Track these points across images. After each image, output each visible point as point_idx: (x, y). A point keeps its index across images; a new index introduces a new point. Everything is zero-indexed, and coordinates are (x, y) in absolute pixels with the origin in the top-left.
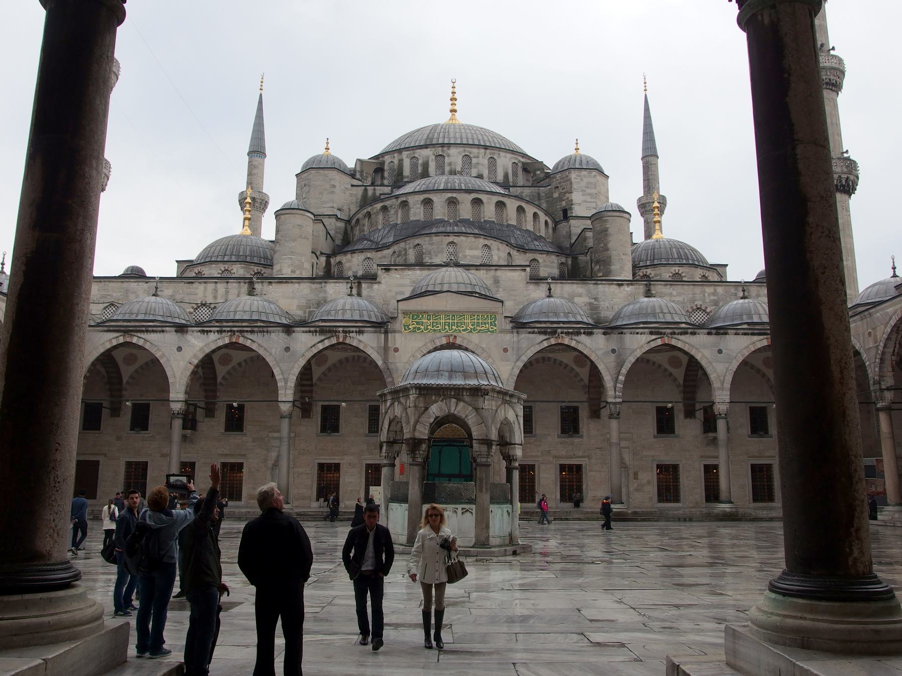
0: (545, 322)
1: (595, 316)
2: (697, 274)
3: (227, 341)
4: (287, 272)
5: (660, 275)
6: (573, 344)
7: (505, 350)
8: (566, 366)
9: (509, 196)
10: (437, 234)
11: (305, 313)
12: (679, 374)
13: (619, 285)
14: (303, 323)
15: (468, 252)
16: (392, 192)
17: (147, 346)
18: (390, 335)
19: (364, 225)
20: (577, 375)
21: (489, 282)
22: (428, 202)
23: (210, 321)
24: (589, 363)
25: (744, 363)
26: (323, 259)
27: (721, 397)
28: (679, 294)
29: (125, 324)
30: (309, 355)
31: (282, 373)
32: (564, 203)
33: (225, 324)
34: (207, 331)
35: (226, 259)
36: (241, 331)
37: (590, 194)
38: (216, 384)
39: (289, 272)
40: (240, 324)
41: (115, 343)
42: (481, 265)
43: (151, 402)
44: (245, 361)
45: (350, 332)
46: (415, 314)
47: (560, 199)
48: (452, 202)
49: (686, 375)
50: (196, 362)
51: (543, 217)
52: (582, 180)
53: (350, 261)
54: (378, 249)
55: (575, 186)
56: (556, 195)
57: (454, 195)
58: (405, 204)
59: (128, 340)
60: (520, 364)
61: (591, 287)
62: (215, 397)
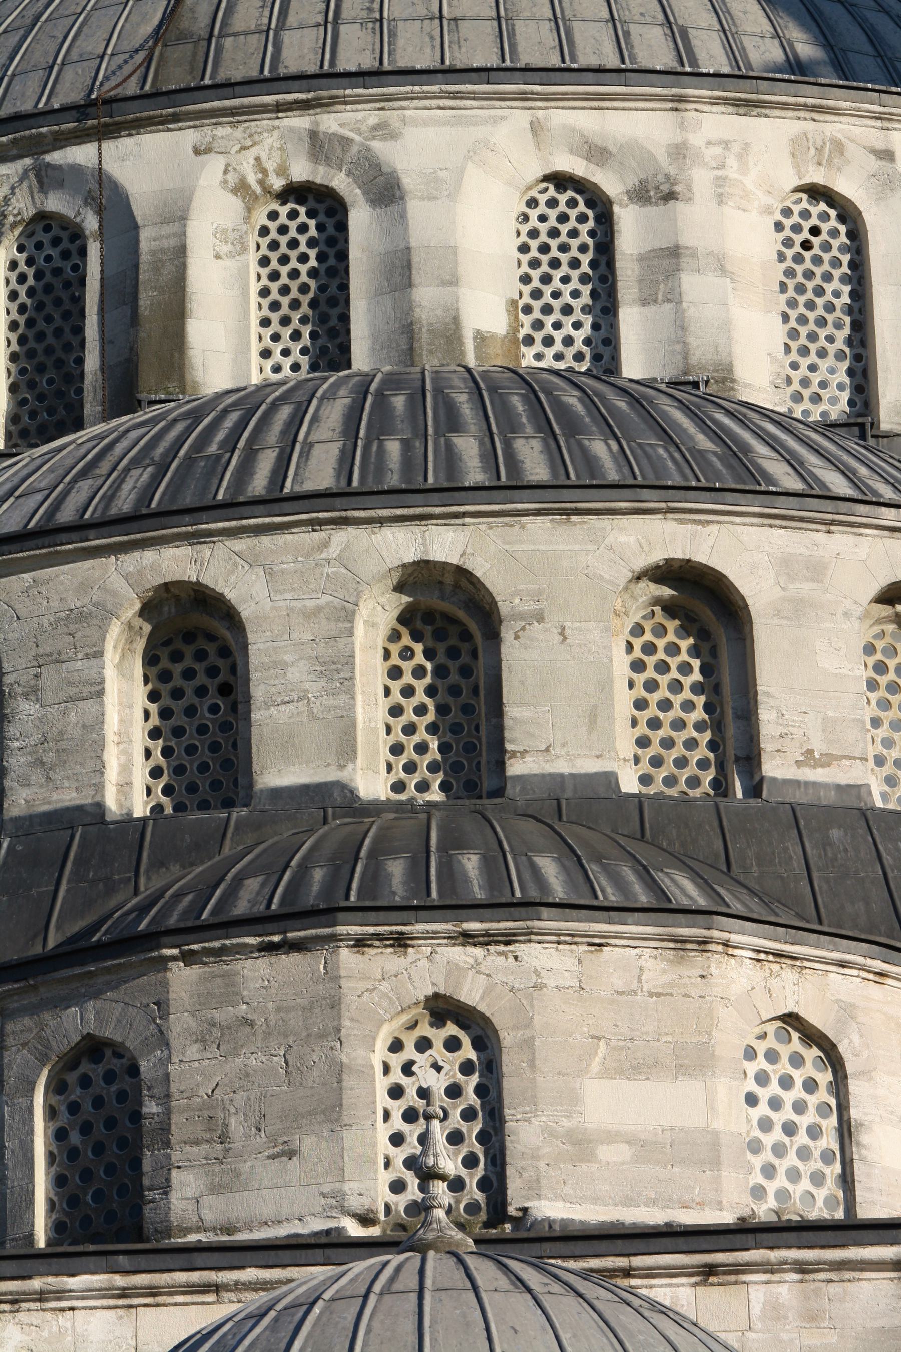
15: (610, 1104)
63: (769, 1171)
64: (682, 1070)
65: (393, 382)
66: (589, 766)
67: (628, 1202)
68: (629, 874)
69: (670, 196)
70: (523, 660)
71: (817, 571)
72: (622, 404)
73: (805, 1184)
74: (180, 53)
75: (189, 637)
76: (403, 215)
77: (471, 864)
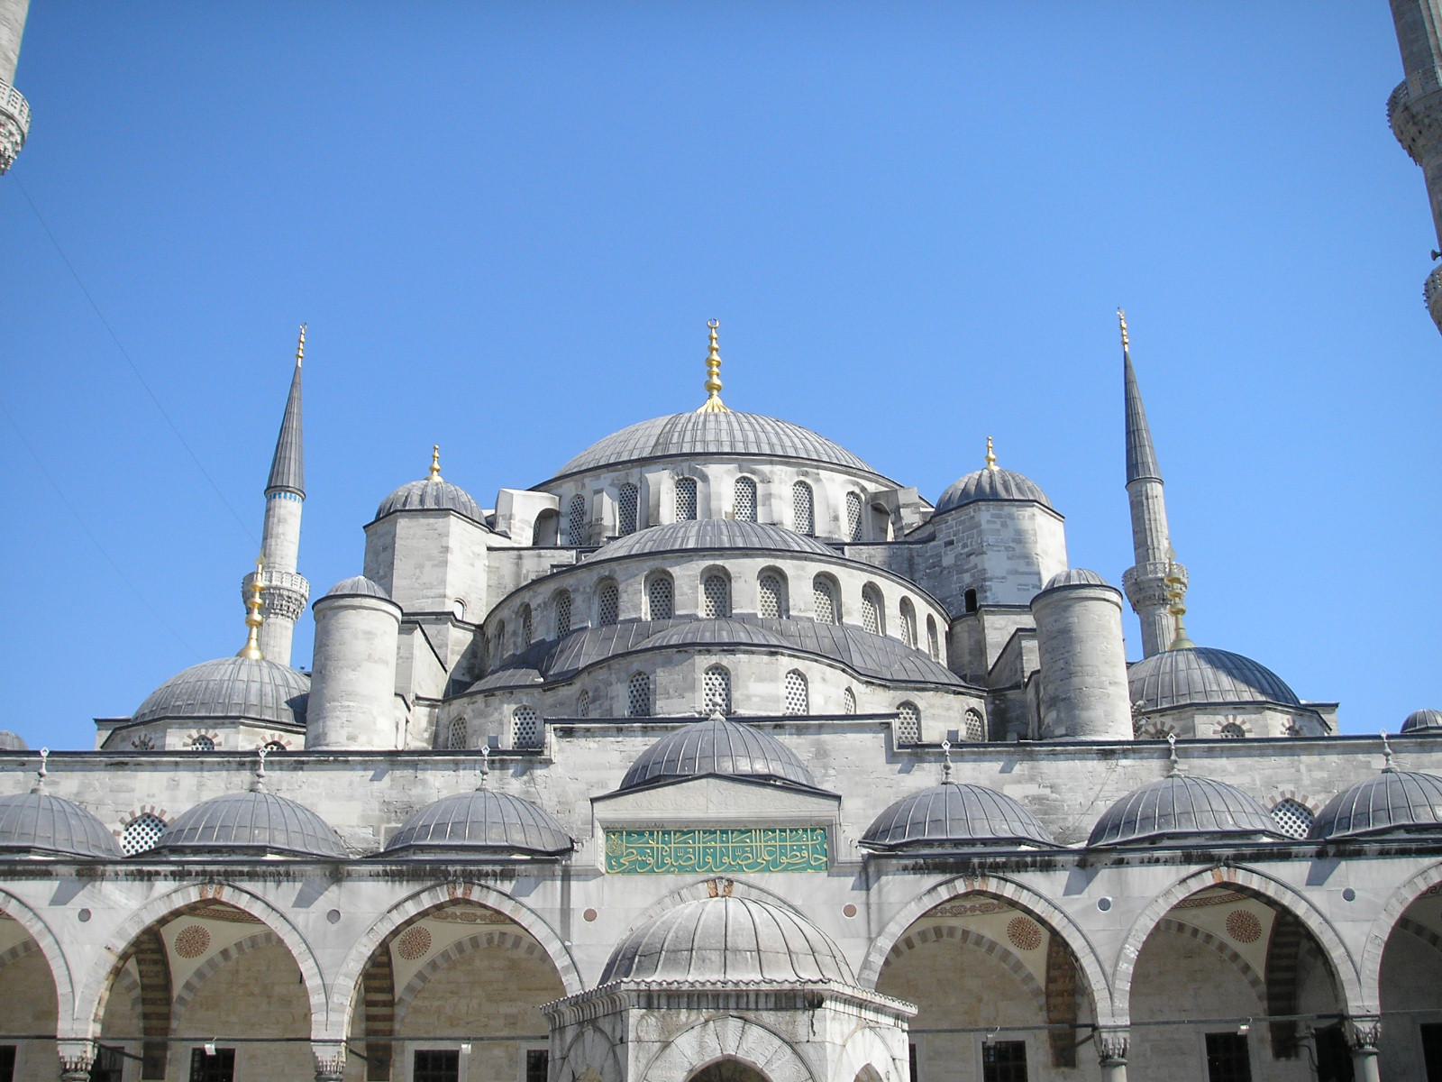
0: (941, 843)
1: (1055, 828)
2: (1277, 723)
3: (193, 895)
4: (338, 739)
5: (1194, 729)
6: (1009, 891)
7: (850, 911)
8: (992, 946)
9: (844, 562)
12: (1256, 954)
14: (372, 858)
18: (574, 884)
20: (1018, 966)
23: (155, 851)
24: (1045, 935)
25: (1403, 922)
26: (421, 713)
27: (1363, 999)
30: (385, 929)
32: (967, 578)
36: (227, 874)
38: (168, 1001)
44: (239, 945)
45: (482, 875)
49: (1271, 957)
50: (121, 945)
51: (922, 608)
52: (1004, 525)
53: (481, 714)
55: (991, 539)
57: (720, 562)
60: (886, 943)
62: (166, 1030)
63: (790, 703)
64: (772, 681)
65: (707, 524)
66: (752, 612)
67: (759, 710)
68: (760, 637)
69: (769, 482)
70: (737, 587)
71: (803, 569)
72: (759, 529)
73: (798, 706)
74: (660, 447)
75: (661, 580)
76: (709, 484)
77: (724, 633)
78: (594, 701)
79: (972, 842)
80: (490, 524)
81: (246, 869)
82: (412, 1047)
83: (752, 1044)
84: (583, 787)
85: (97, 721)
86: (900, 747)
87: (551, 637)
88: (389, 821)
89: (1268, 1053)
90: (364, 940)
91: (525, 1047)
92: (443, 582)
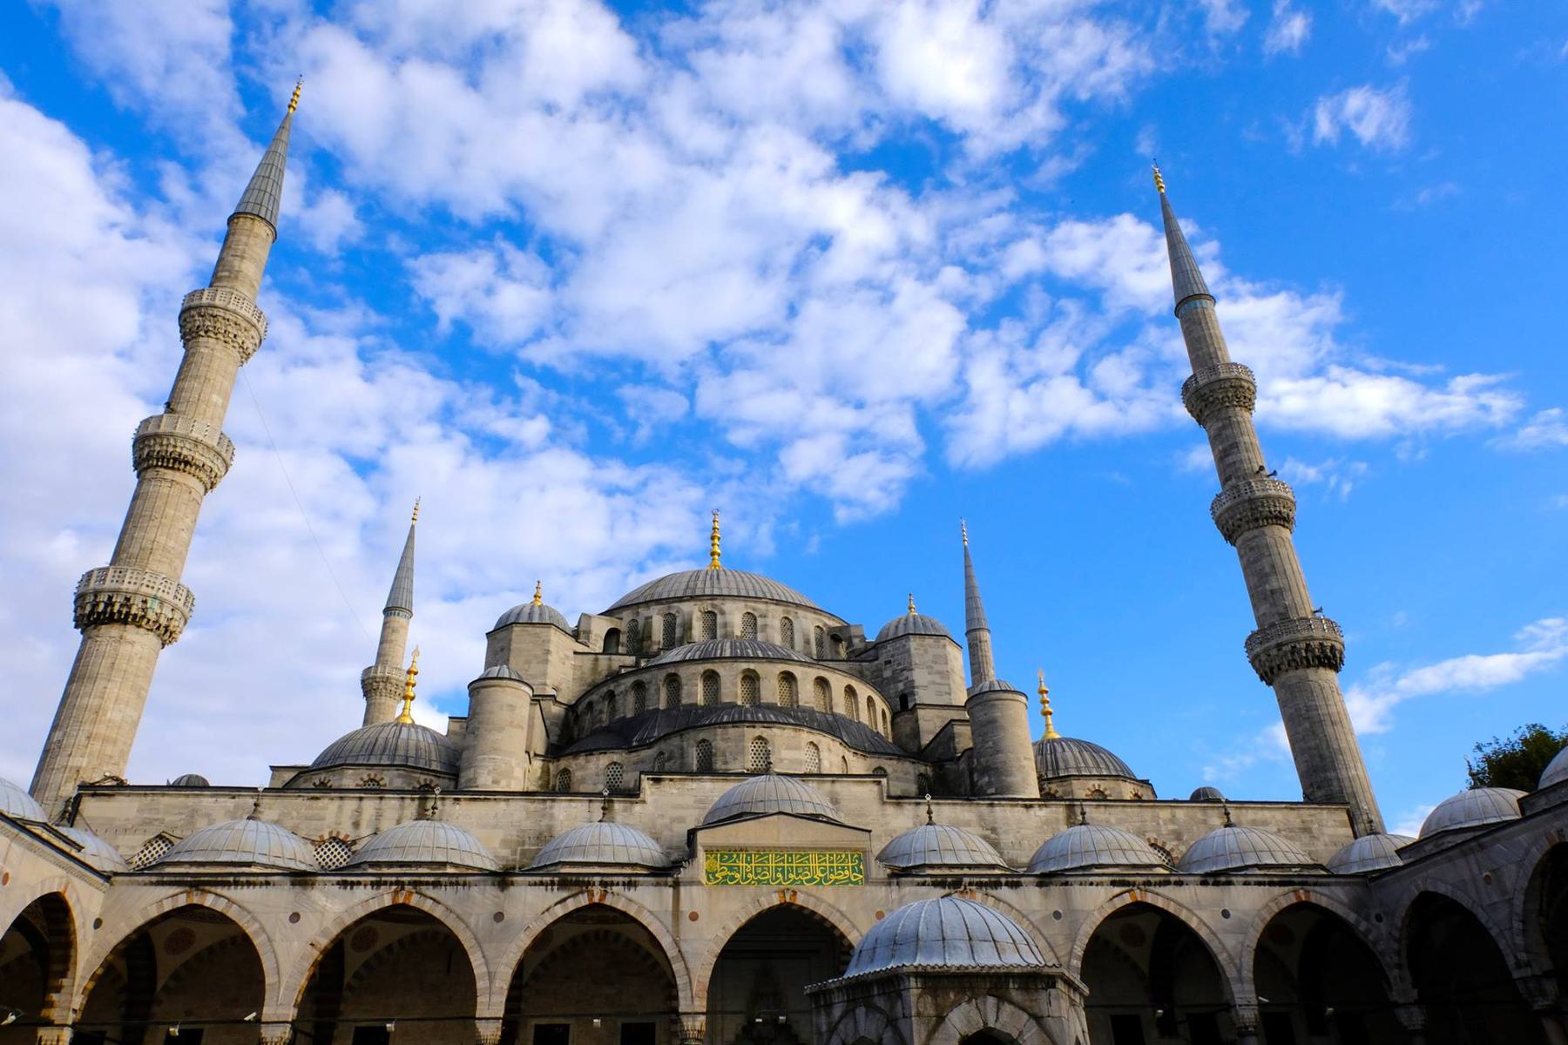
2: (1128, 790)
3: (387, 901)
4: (485, 782)
10: (735, 723)
11: (514, 853)
12: (1141, 956)
13: (1027, 807)
15: (785, 754)
16: (637, 663)
17: (232, 913)
18: (682, 889)
19: (601, 712)
21: (826, 802)
22: (711, 678)
23: (358, 866)
26: (538, 763)
28: (1120, 822)
29: (194, 870)
30: (538, 927)
31: (487, 964)
32: (901, 686)
33: (385, 870)
34: (352, 884)
35: (373, 761)
36: (415, 884)
37: (939, 673)
39: (489, 782)
40: (413, 870)
41: (168, 906)
42: (805, 775)
43: (206, 1027)
44: (401, 942)
45: (612, 884)
46: (725, 853)
47: (894, 679)
48: (751, 678)
50: (324, 942)
51: (880, 705)
53: (583, 768)
54: (631, 750)
55: (916, 660)
56: (887, 673)
57: (752, 666)
58: (673, 681)
59: (196, 900)
61: (985, 810)
78: (670, 759)
79: (961, 866)
80: (576, 635)
81: (431, 879)
82: (534, 1022)
83: (1006, 1019)
84: (667, 821)
85: (272, 768)
86: (889, 797)
87: (629, 715)
88: (523, 843)
89: (1155, 1033)
90: (522, 936)
91: (620, 1022)
92: (545, 674)
